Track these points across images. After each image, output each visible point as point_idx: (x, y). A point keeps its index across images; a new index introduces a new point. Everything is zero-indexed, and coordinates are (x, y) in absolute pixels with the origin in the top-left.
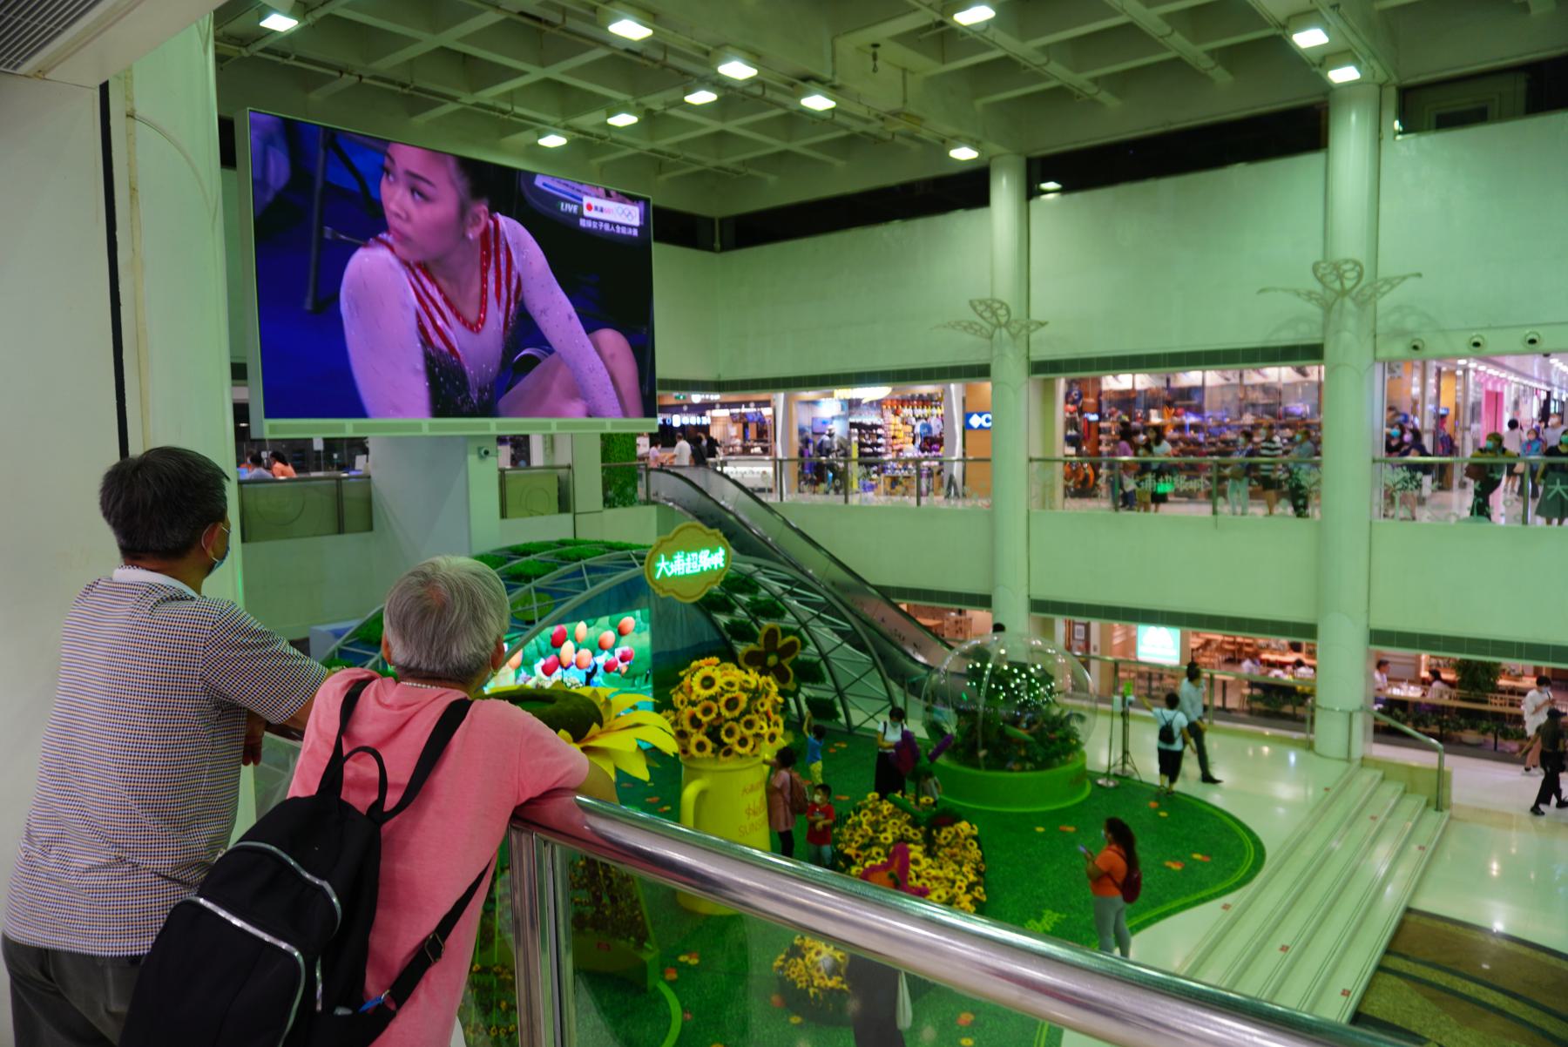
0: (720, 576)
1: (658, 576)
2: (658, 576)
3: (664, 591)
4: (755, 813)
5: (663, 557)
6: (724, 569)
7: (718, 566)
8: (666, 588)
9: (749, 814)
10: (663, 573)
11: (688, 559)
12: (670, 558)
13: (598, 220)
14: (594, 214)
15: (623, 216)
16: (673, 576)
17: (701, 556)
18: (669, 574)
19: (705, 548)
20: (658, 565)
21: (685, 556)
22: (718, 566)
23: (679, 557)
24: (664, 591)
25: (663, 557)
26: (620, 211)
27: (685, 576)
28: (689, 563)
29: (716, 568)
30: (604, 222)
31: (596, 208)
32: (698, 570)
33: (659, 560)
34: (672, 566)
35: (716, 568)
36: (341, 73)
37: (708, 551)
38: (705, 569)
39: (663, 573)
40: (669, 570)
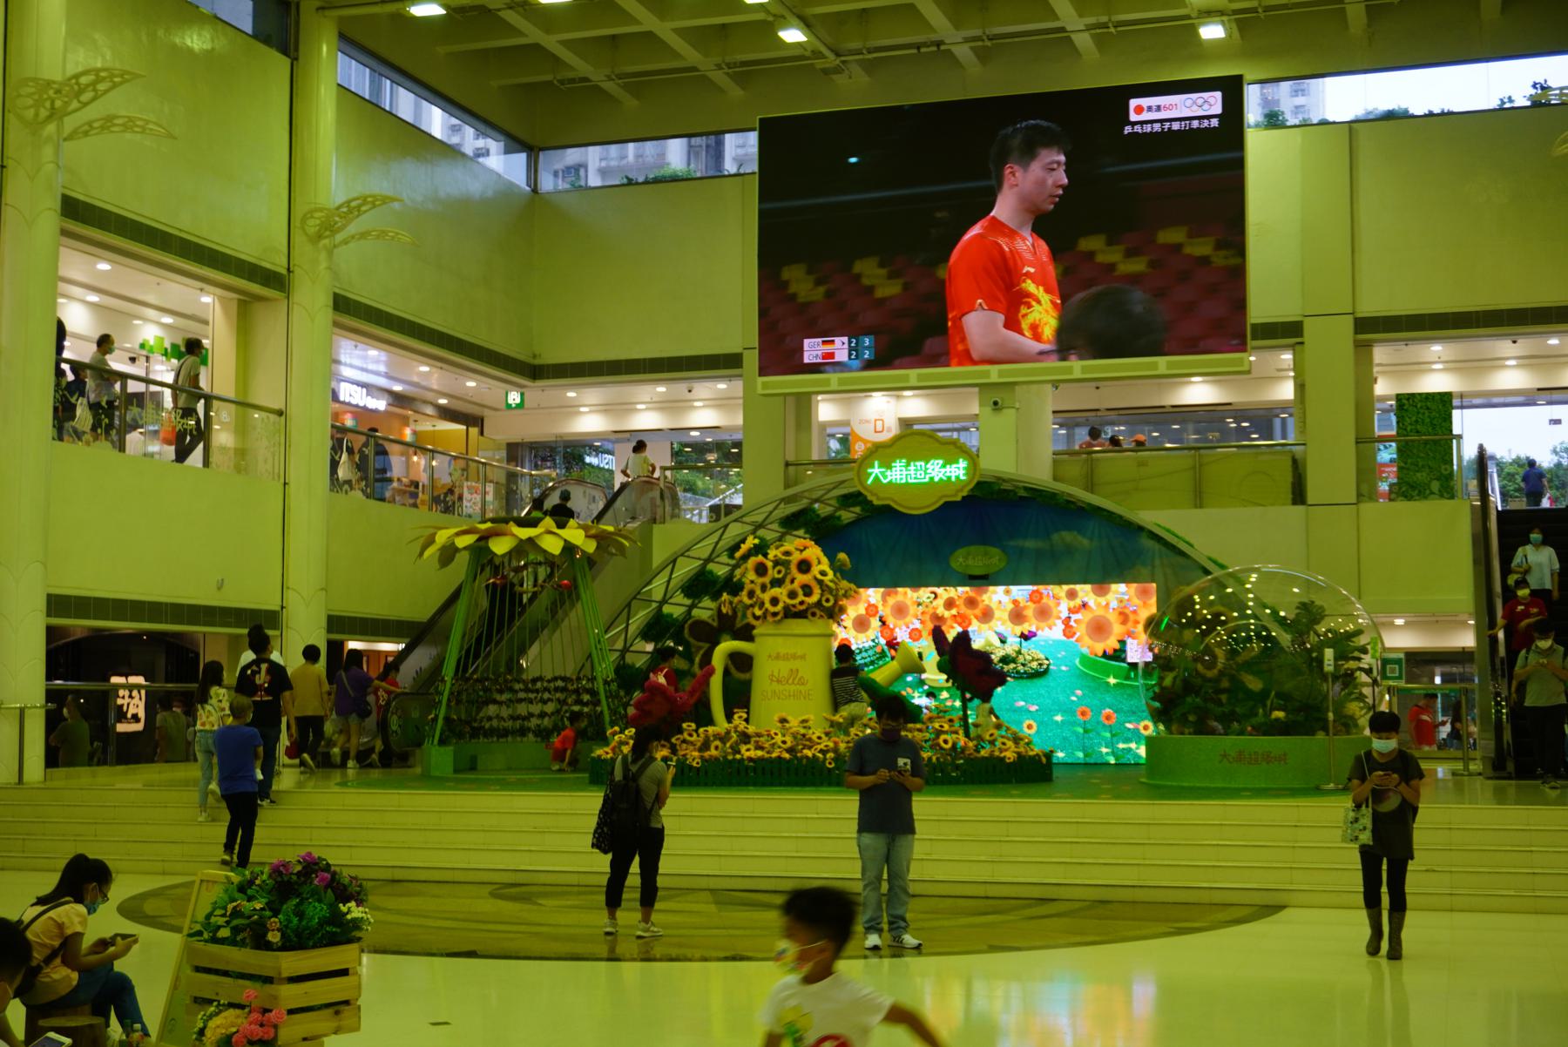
0: (962, 490)
1: (870, 481)
2: (870, 481)
3: (878, 498)
4: (779, 681)
5: (876, 463)
6: (966, 484)
7: (957, 478)
8: (881, 495)
9: (772, 680)
10: (877, 478)
11: (912, 467)
12: (887, 465)
13: (1161, 121)
14: (1146, 116)
15: (1195, 108)
16: (890, 482)
17: (929, 465)
18: (884, 481)
19: (937, 457)
20: (869, 471)
21: (908, 464)
22: (957, 478)
23: (899, 465)
24: (878, 498)
25: (876, 463)
26: (1189, 103)
27: (907, 485)
28: (912, 472)
29: (953, 479)
30: (1170, 120)
31: (1150, 109)
32: (927, 480)
33: (873, 467)
34: (889, 473)
35: (953, 479)
36: (918, 48)
37: (941, 462)
38: (936, 479)
39: (877, 478)
40: (886, 477)
